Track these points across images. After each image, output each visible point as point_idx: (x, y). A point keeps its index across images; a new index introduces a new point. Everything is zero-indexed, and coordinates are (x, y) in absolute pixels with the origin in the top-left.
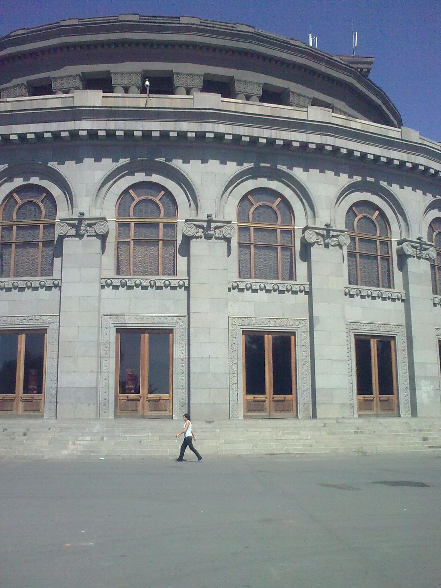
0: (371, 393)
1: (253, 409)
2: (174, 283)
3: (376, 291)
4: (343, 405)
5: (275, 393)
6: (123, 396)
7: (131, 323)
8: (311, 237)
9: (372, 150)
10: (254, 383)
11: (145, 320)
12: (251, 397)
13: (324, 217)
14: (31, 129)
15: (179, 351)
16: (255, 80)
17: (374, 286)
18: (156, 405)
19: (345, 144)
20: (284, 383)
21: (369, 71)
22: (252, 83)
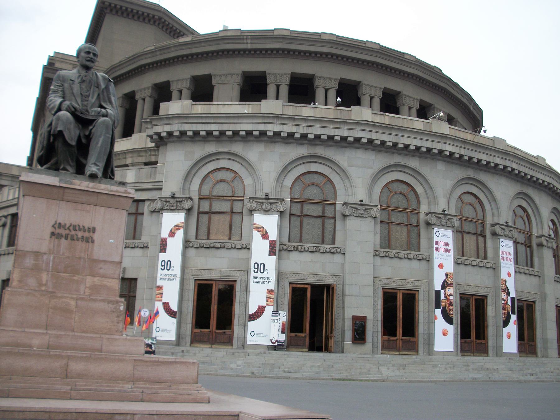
2: (488, 265)
7: (468, 290)
11: (479, 290)
14: (414, 142)
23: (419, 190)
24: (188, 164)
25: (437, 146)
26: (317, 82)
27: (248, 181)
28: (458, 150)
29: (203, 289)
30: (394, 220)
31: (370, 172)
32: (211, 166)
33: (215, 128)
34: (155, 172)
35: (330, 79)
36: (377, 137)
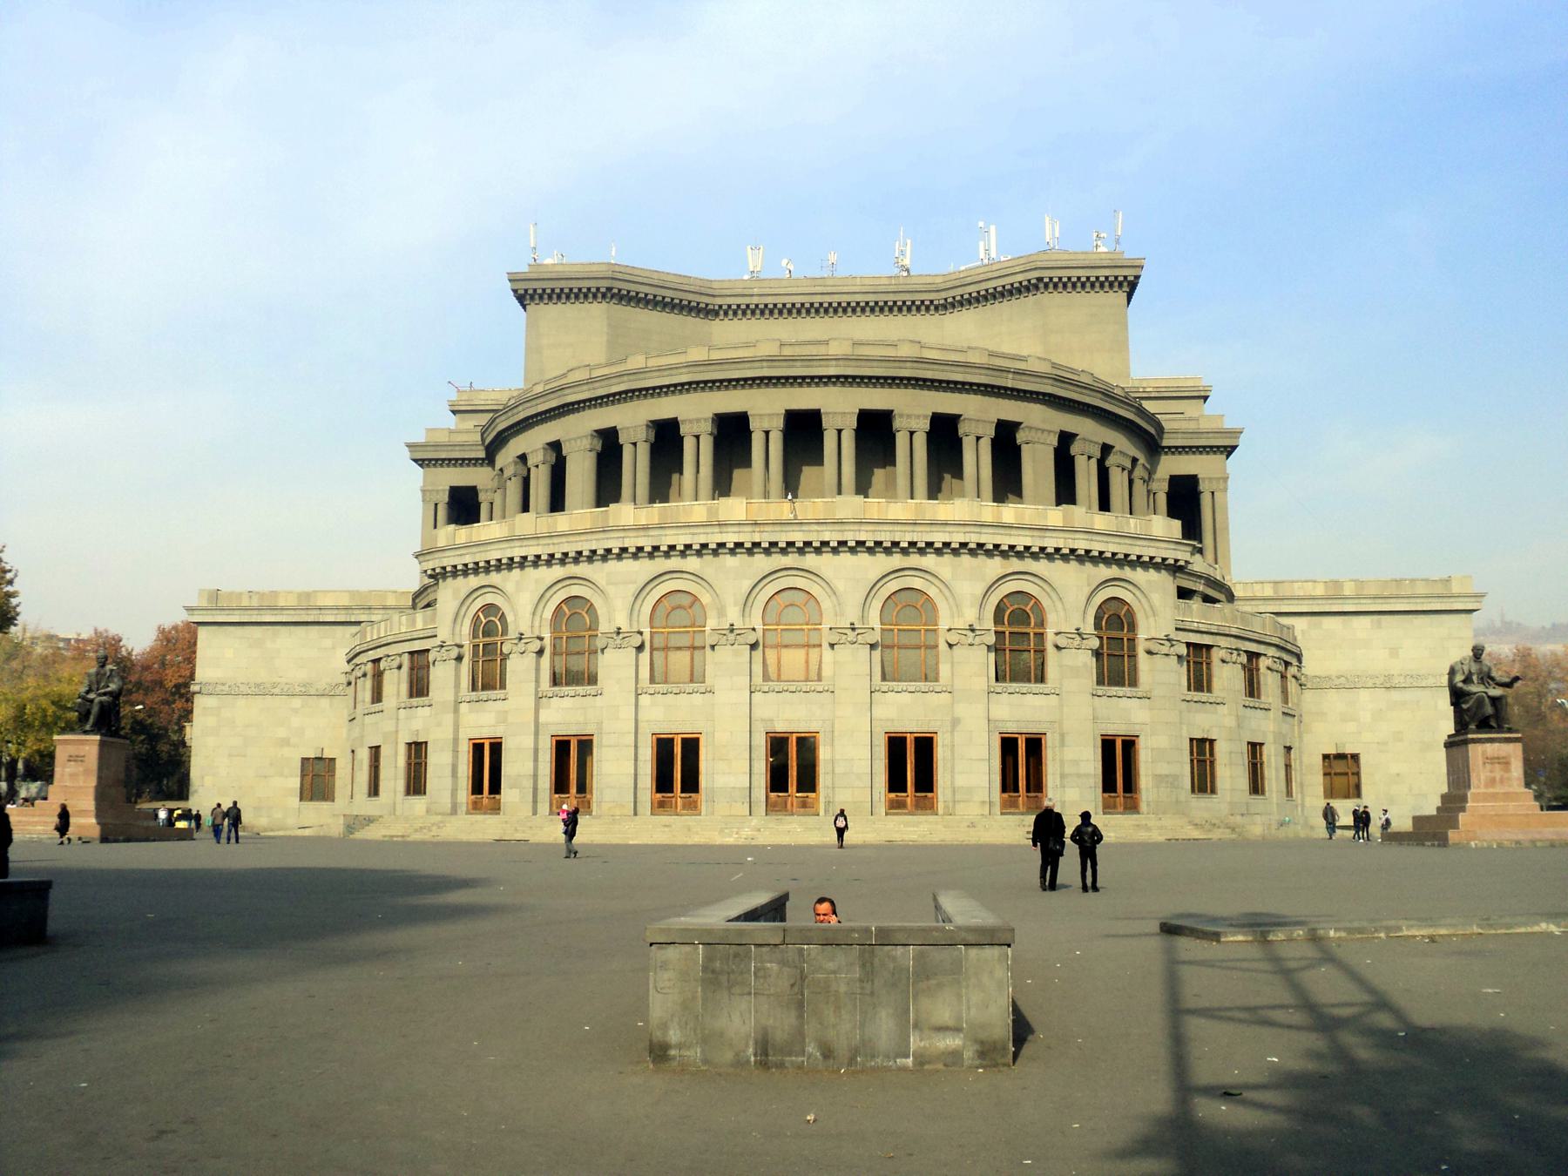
0: (1016, 790)
1: (895, 806)
3: (1024, 687)
4: (983, 802)
5: (917, 790)
6: (773, 795)
7: (780, 727)
8: (953, 638)
9: (1021, 541)
10: (896, 782)
12: (893, 795)
13: (969, 615)
14: (680, 540)
15: (823, 754)
16: (921, 412)
17: (1022, 681)
18: (804, 805)
19: (989, 539)
20: (926, 782)
21: (1137, 277)
22: (918, 417)
23: (705, 598)
24: (457, 604)
25: (713, 539)
26: (684, 430)
27: (510, 618)
28: (747, 538)
29: (478, 748)
30: (671, 644)
31: (633, 589)
32: (479, 604)
33: (468, 559)
34: (434, 615)
35: (698, 420)
36: (631, 543)
